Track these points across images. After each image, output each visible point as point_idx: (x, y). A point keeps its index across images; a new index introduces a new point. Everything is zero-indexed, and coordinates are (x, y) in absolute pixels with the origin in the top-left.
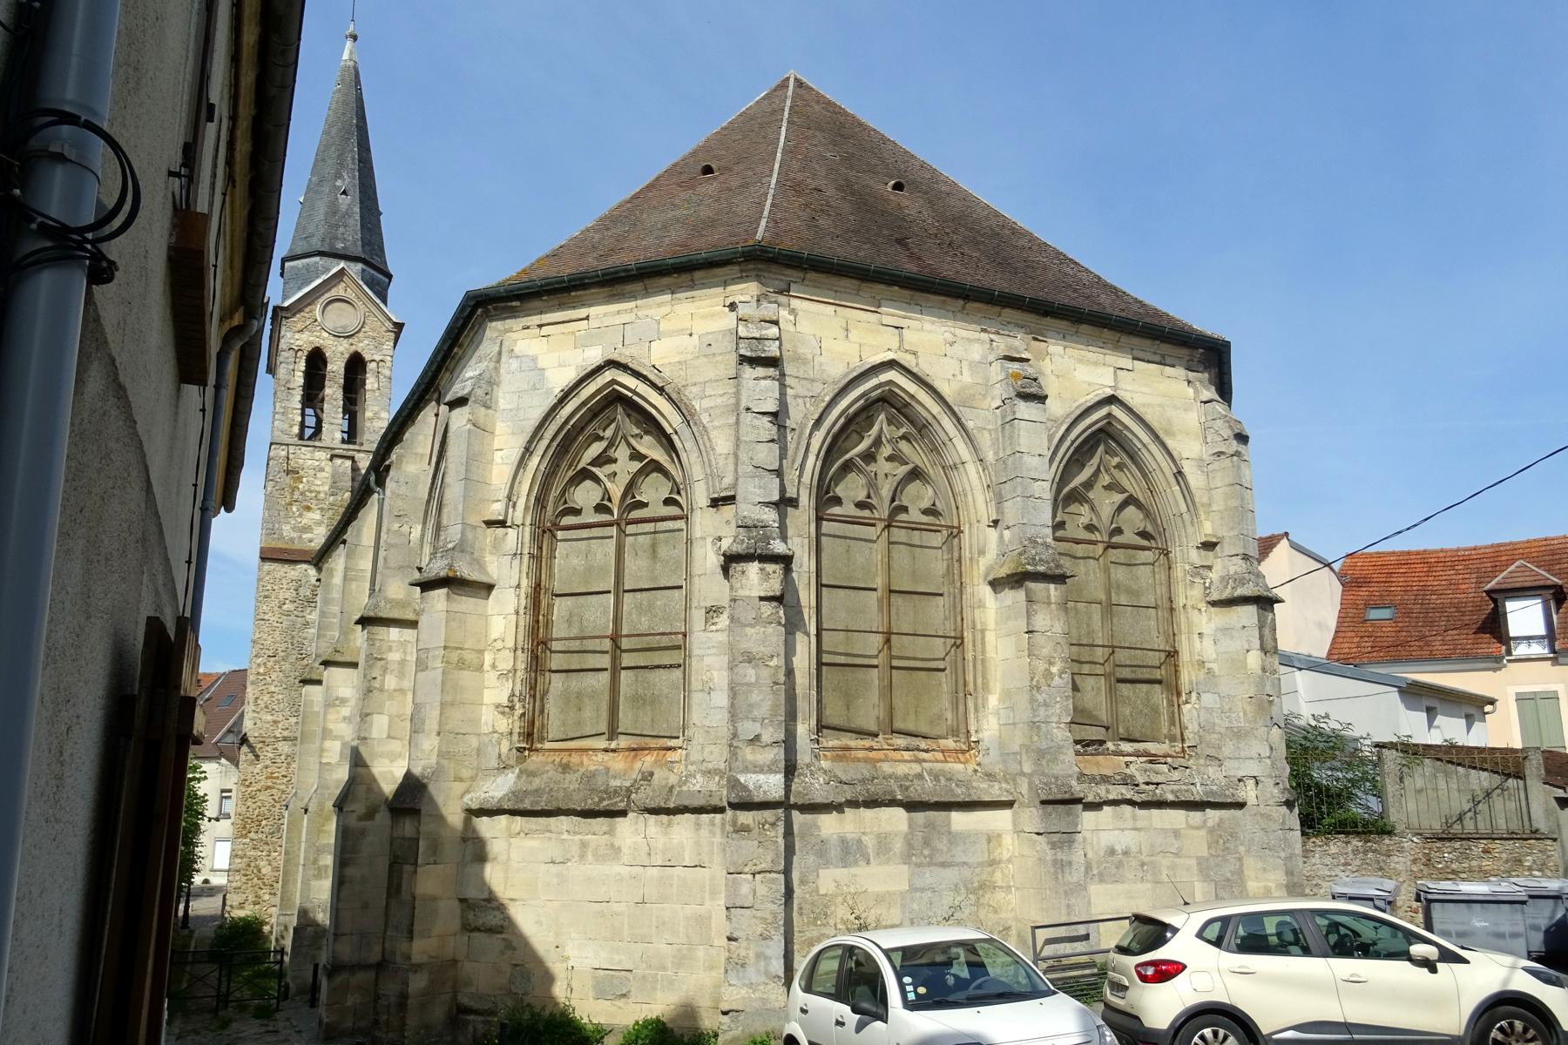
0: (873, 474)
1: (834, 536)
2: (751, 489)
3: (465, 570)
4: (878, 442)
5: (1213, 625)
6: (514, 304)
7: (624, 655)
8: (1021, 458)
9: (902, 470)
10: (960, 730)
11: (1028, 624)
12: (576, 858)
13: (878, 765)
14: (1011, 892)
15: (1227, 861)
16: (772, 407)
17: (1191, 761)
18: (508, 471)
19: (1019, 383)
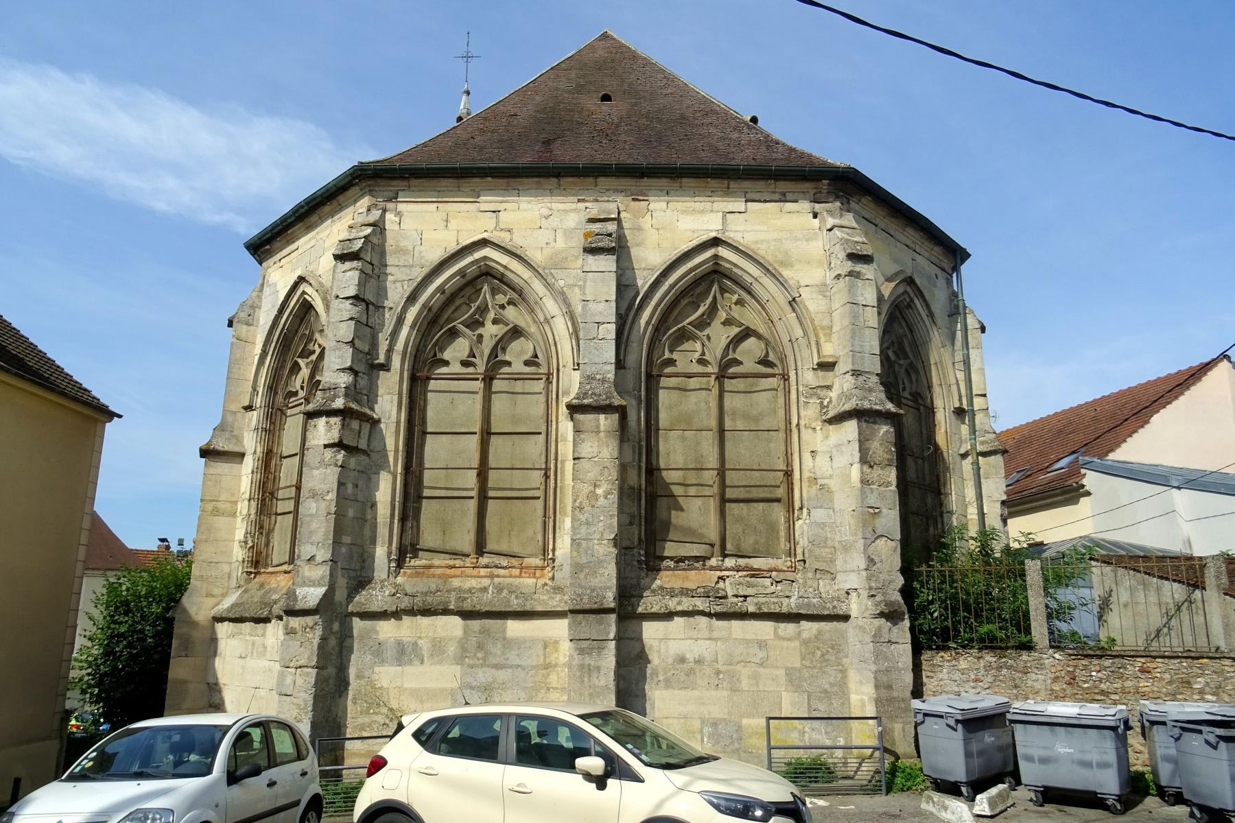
1: (440, 392)
16: (352, 291)
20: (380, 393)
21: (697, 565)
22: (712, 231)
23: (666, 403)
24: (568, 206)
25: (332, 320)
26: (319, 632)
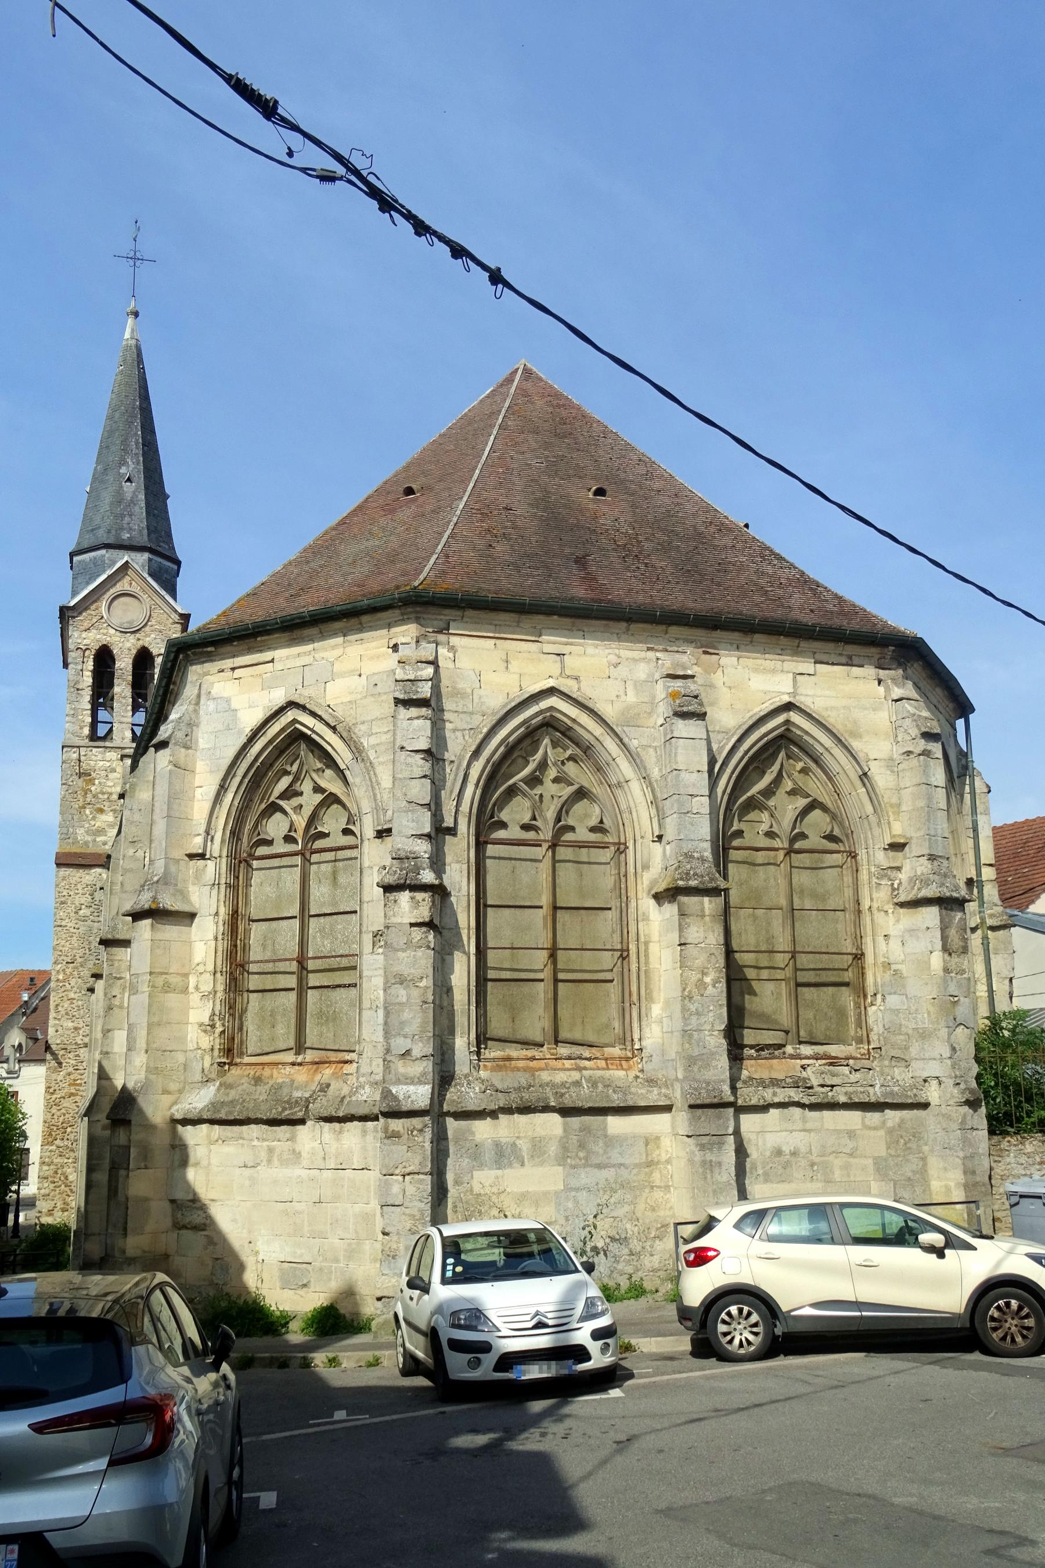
0: (537, 797)
1: (500, 858)
2: (405, 822)
3: (168, 902)
4: (543, 765)
5: (901, 926)
6: (209, 649)
7: (310, 975)
8: (678, 776)
9: (568, 791)
10: (624, 1039)
11: (680, 937)
12: (265, 1163)
13: (537, 1073)
14: (669, 1192)
15: (908, 1160)
16: (424, 744)
17: (875, 1062)
18: (207, 806)
19: (678, 701)
20: (449, 859)
21: (777, 1053)
22: (783, 693)
23: (736, 879)
24: (636, 654)
25: (400, 776)
26: (428, 1134)
